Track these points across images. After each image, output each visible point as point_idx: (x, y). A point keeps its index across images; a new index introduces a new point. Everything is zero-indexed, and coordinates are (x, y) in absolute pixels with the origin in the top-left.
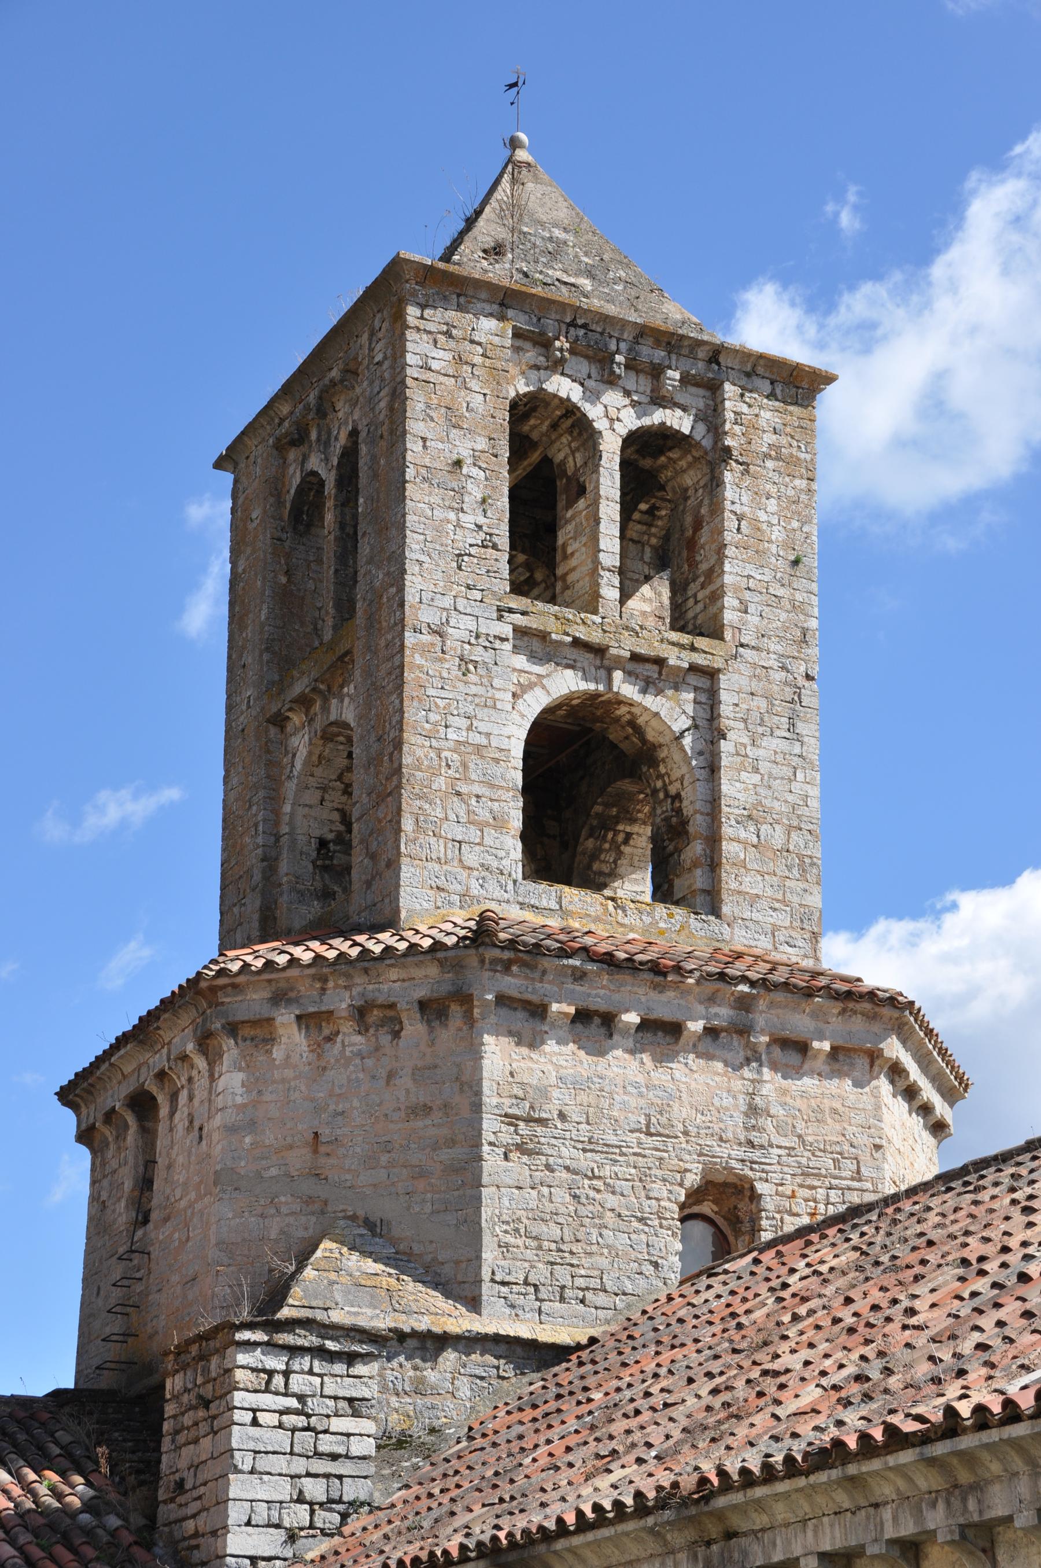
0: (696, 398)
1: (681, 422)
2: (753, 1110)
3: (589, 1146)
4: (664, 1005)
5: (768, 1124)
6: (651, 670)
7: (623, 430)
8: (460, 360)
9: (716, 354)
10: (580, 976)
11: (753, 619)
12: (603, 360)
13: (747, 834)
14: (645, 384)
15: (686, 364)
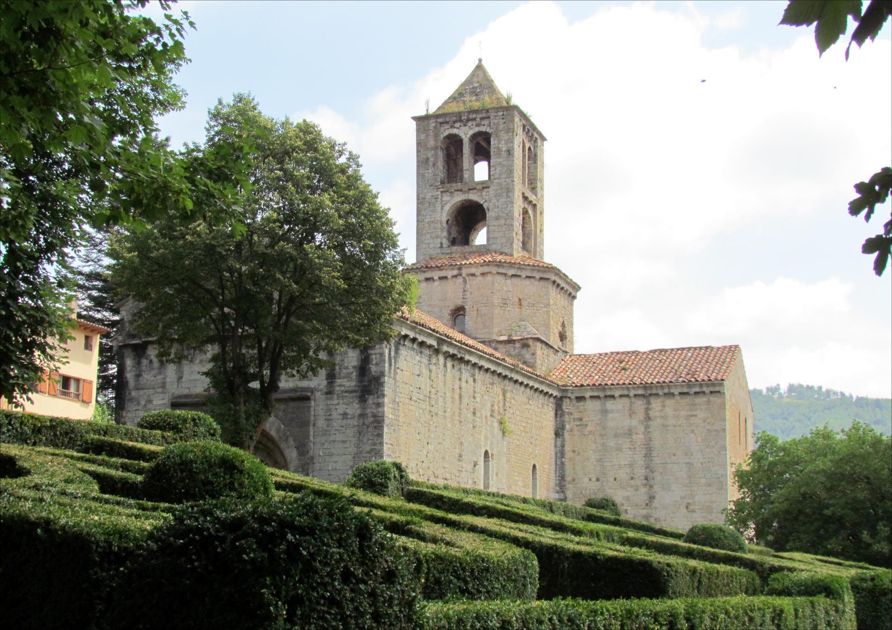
0: (486, 122)
1: (483, 129)
2: (464, 291)
3: (430, 306)
4: (443, 274)
5: (468, 293)
6: (475, 191)
7: (468, 136)
8: (427, 136)
9: (487, 111)
10: (424, 272)
11: (498, 171)
12: (461, 121)
13: (496, 223)
14: (474, 123)
15: (480, 116)
